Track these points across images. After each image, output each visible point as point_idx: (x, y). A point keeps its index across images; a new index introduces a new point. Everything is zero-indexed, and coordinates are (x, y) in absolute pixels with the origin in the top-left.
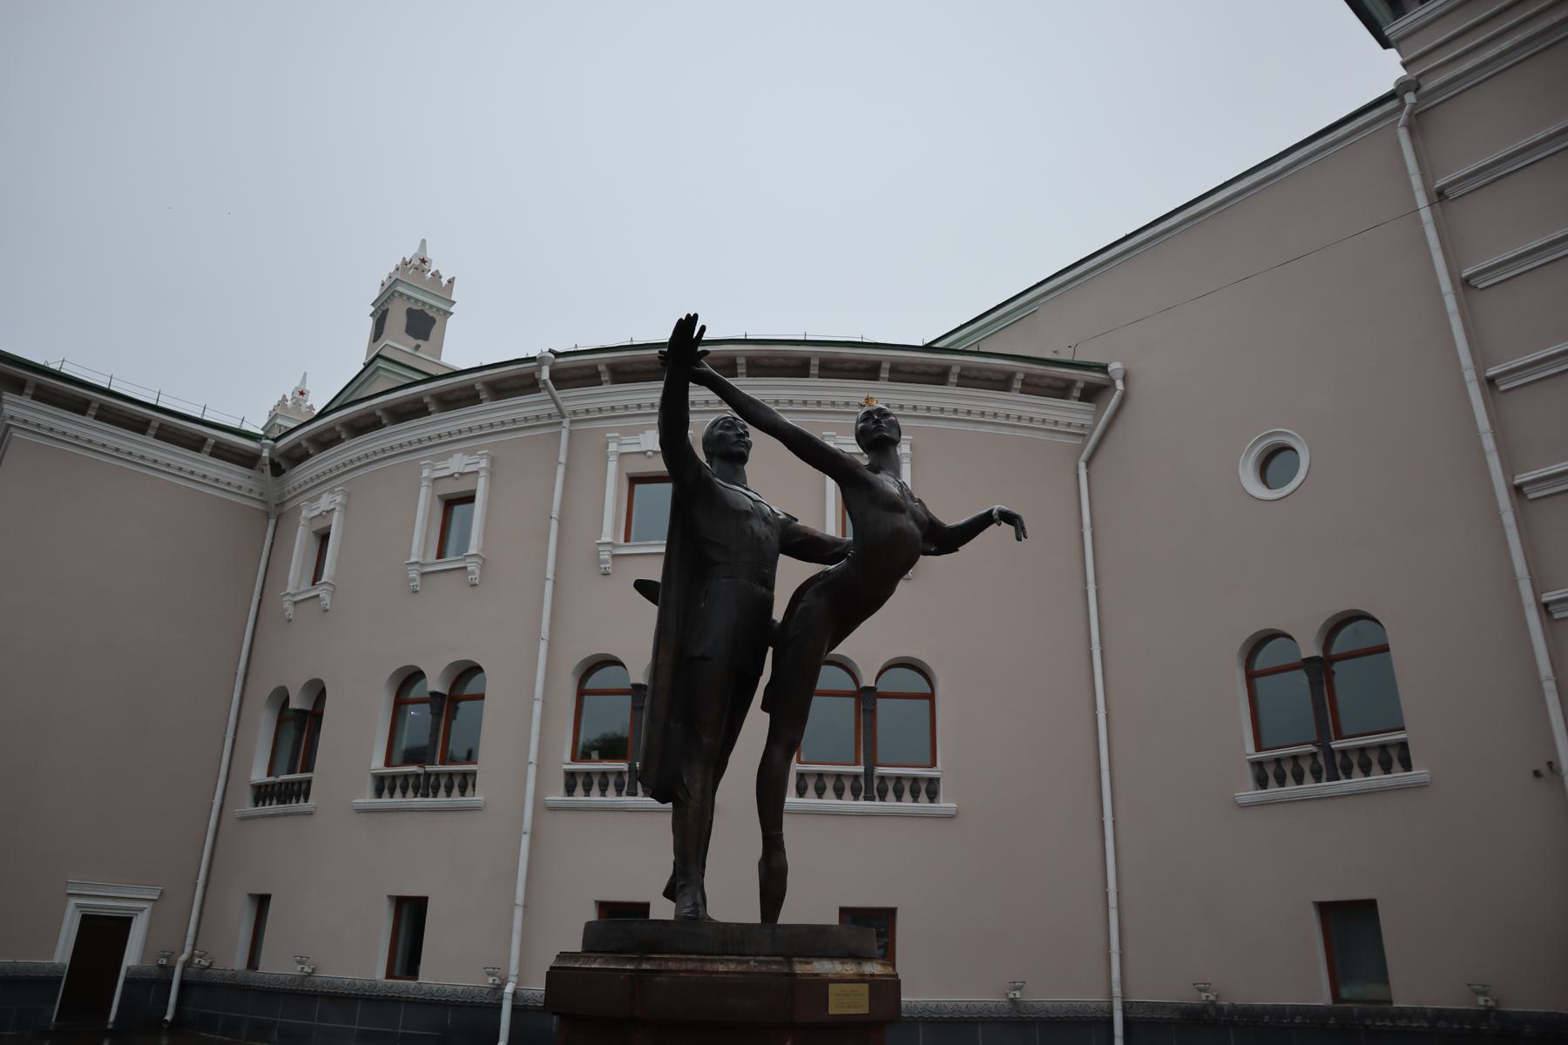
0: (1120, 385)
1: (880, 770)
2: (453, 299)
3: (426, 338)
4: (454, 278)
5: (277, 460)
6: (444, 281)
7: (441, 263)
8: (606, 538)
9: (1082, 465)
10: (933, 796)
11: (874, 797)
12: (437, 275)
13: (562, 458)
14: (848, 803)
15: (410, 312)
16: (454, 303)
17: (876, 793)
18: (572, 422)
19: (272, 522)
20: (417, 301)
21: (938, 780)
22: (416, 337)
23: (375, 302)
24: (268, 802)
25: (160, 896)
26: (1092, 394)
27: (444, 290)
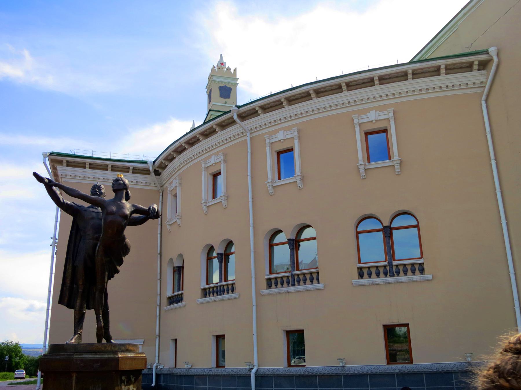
0: (495, 59)
1: (395, 263)
2: (237, 77)
3: (228, 96)
4: (236, 68)
5: (157, 169)
6: (232, 71)
7: (230, 64)
9: (483, 102)
10: (422, 271)
11: (394, 275)
12: (229, 69)
13: (249, 150)
14: (382, 279)
15: (221, 88)
16: (238, 79)
17: (395, 273)
18: (251, 133)
19: (161, 194)
21: (423, 263)
23: (207, 87)
24: (173, 303)
25: (143, 343)
26: (483, 65)
27: (233, 76)
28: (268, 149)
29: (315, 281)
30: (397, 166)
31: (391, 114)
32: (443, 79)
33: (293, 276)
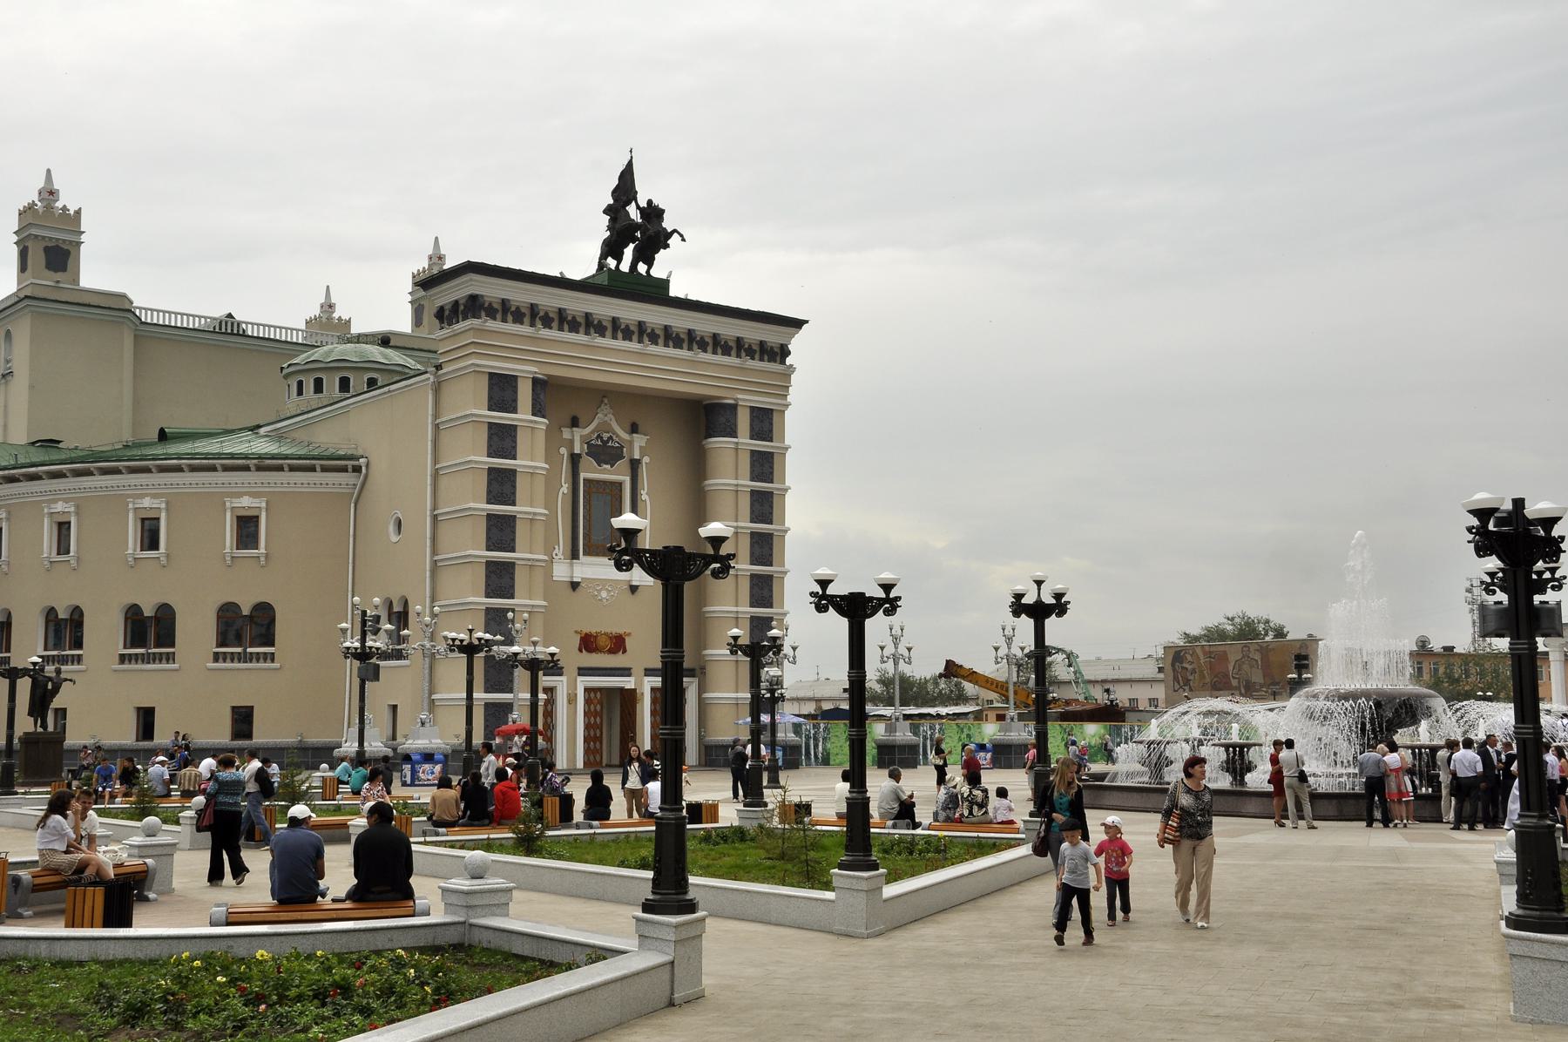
2: (82, 230)
3: (64, 269)
6: (72, 212)
7: (68, 200)
8: (130, 551)
9: (353, 505)
10: (273, 660)
12: (64, 208)
14: (236, 665)
15: (47, 250)
20: (51, 239)
22: (56, 270)
26: (357, 469)
27: (73, 220)
28: (131, 515)
29: (171, 661)
30: (262, 559)
31: (264, 505)
32: (318, 477)
33: (149, 654)
